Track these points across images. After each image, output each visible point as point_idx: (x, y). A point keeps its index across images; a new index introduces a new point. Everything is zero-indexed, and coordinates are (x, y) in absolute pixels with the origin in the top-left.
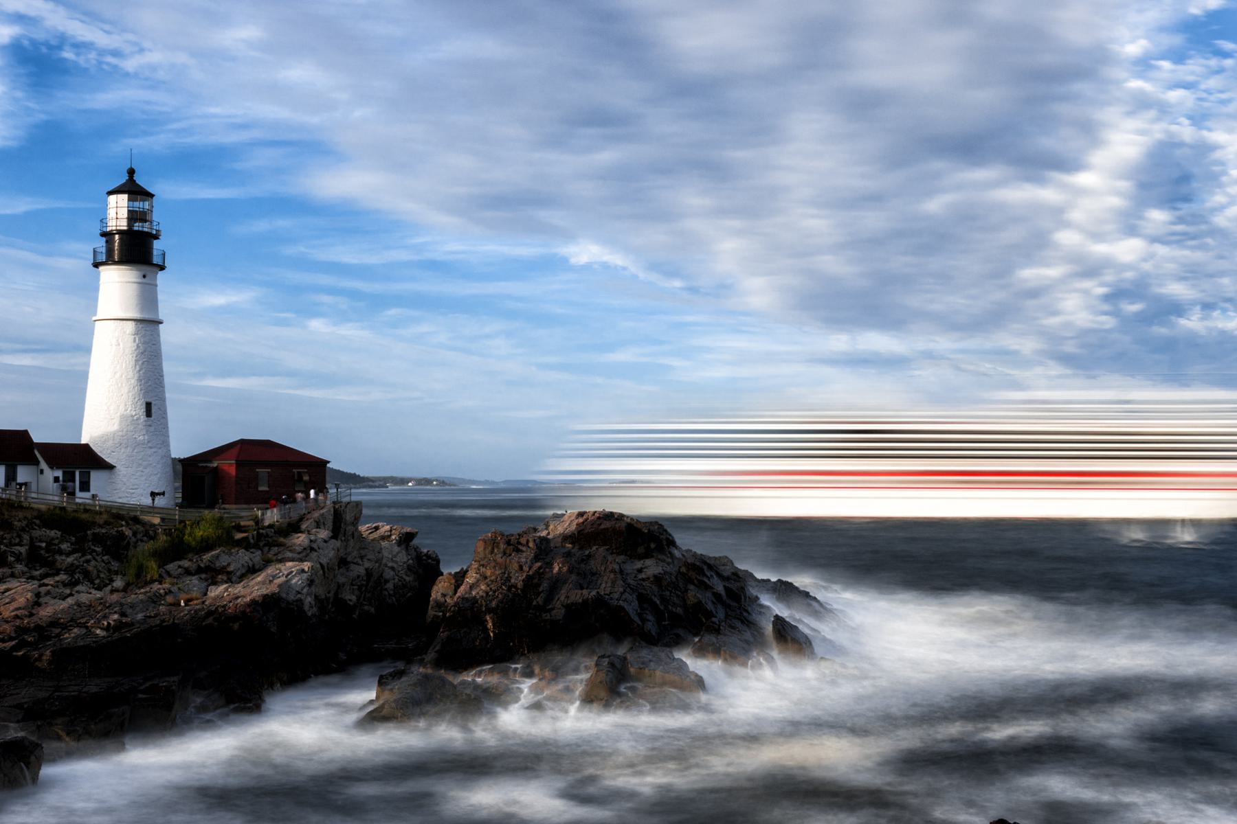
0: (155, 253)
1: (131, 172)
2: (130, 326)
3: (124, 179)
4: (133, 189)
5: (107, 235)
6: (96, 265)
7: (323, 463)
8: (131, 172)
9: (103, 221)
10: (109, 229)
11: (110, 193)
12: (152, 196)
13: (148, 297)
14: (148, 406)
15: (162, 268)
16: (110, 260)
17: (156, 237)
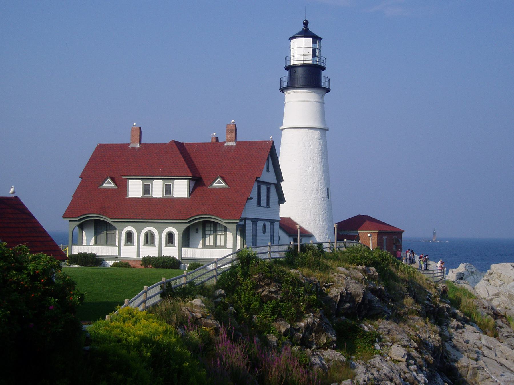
0: (324, 80)
1: (306, 23)
2: (317, 134)
3: (301, 27)
4: (306, 33)
5: (291, 69)
6: (282, 90)
7: (399, 233)
8: (306, 23)
9: (288, 58)
10: (292, 63)
11: (293, 37)
12: (320, 39)
13: (323, 114)
14: (328, 189)
15: (328, 90)
16: (292, 85)
17: (323, 69)
